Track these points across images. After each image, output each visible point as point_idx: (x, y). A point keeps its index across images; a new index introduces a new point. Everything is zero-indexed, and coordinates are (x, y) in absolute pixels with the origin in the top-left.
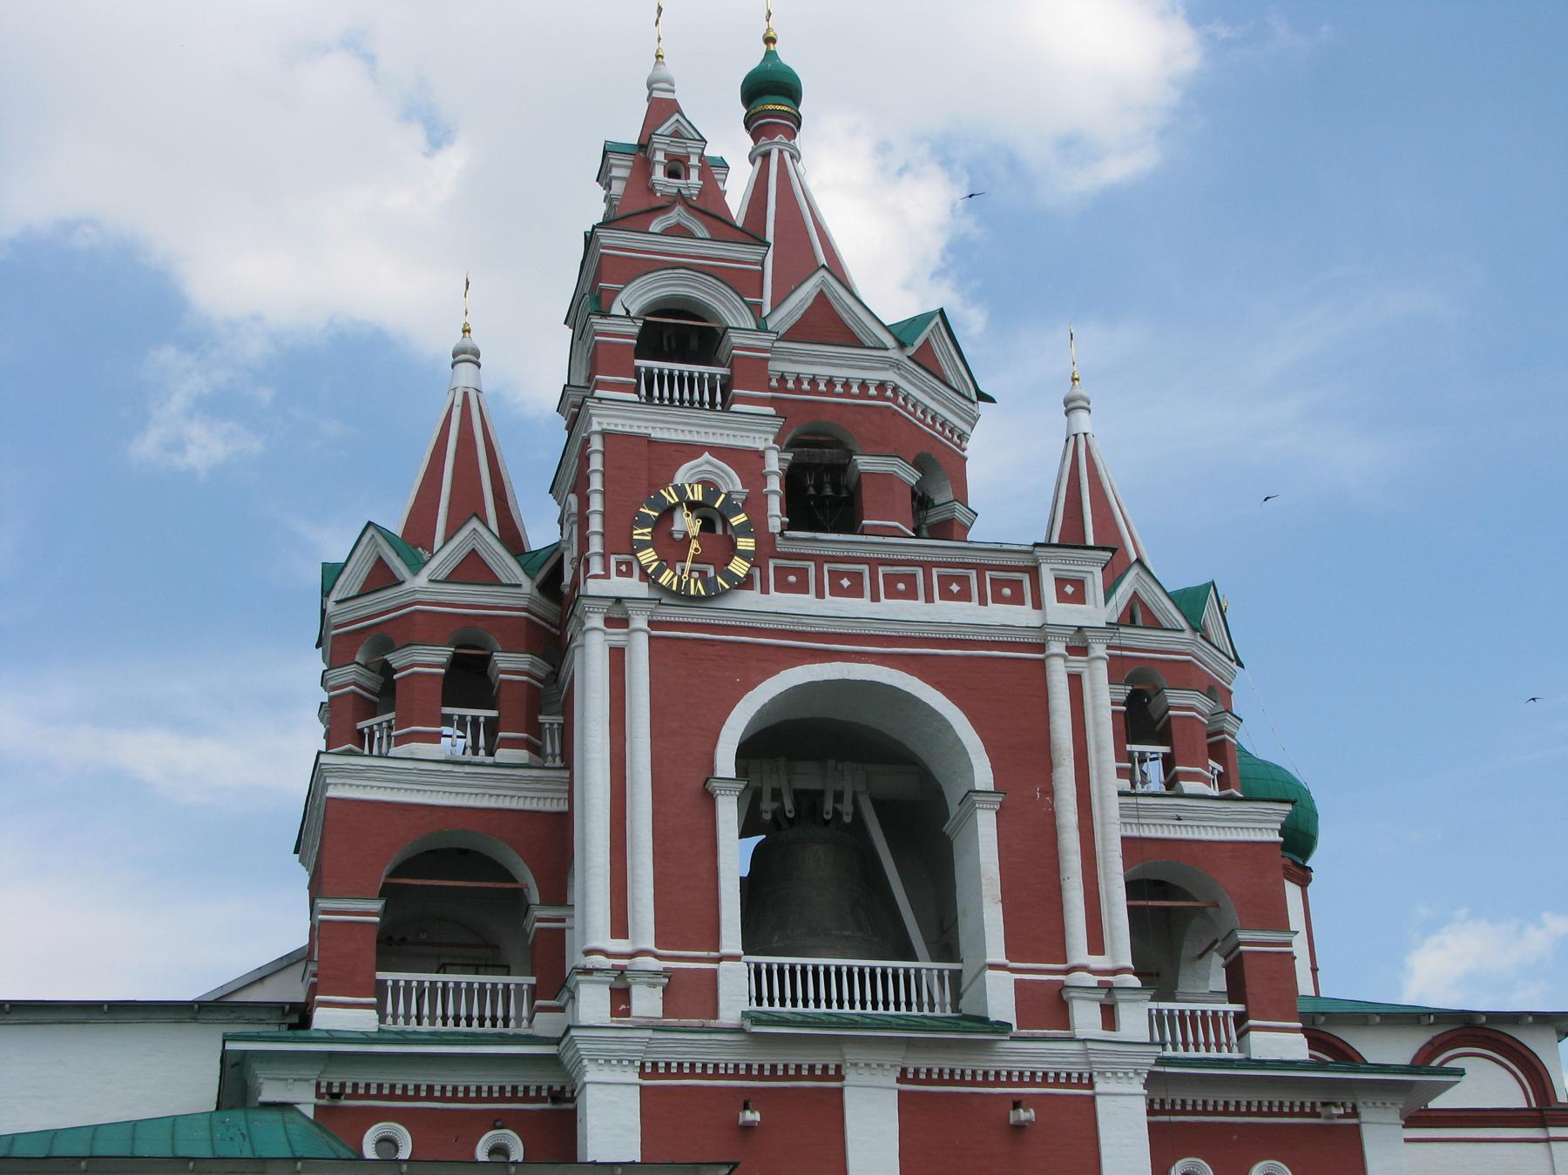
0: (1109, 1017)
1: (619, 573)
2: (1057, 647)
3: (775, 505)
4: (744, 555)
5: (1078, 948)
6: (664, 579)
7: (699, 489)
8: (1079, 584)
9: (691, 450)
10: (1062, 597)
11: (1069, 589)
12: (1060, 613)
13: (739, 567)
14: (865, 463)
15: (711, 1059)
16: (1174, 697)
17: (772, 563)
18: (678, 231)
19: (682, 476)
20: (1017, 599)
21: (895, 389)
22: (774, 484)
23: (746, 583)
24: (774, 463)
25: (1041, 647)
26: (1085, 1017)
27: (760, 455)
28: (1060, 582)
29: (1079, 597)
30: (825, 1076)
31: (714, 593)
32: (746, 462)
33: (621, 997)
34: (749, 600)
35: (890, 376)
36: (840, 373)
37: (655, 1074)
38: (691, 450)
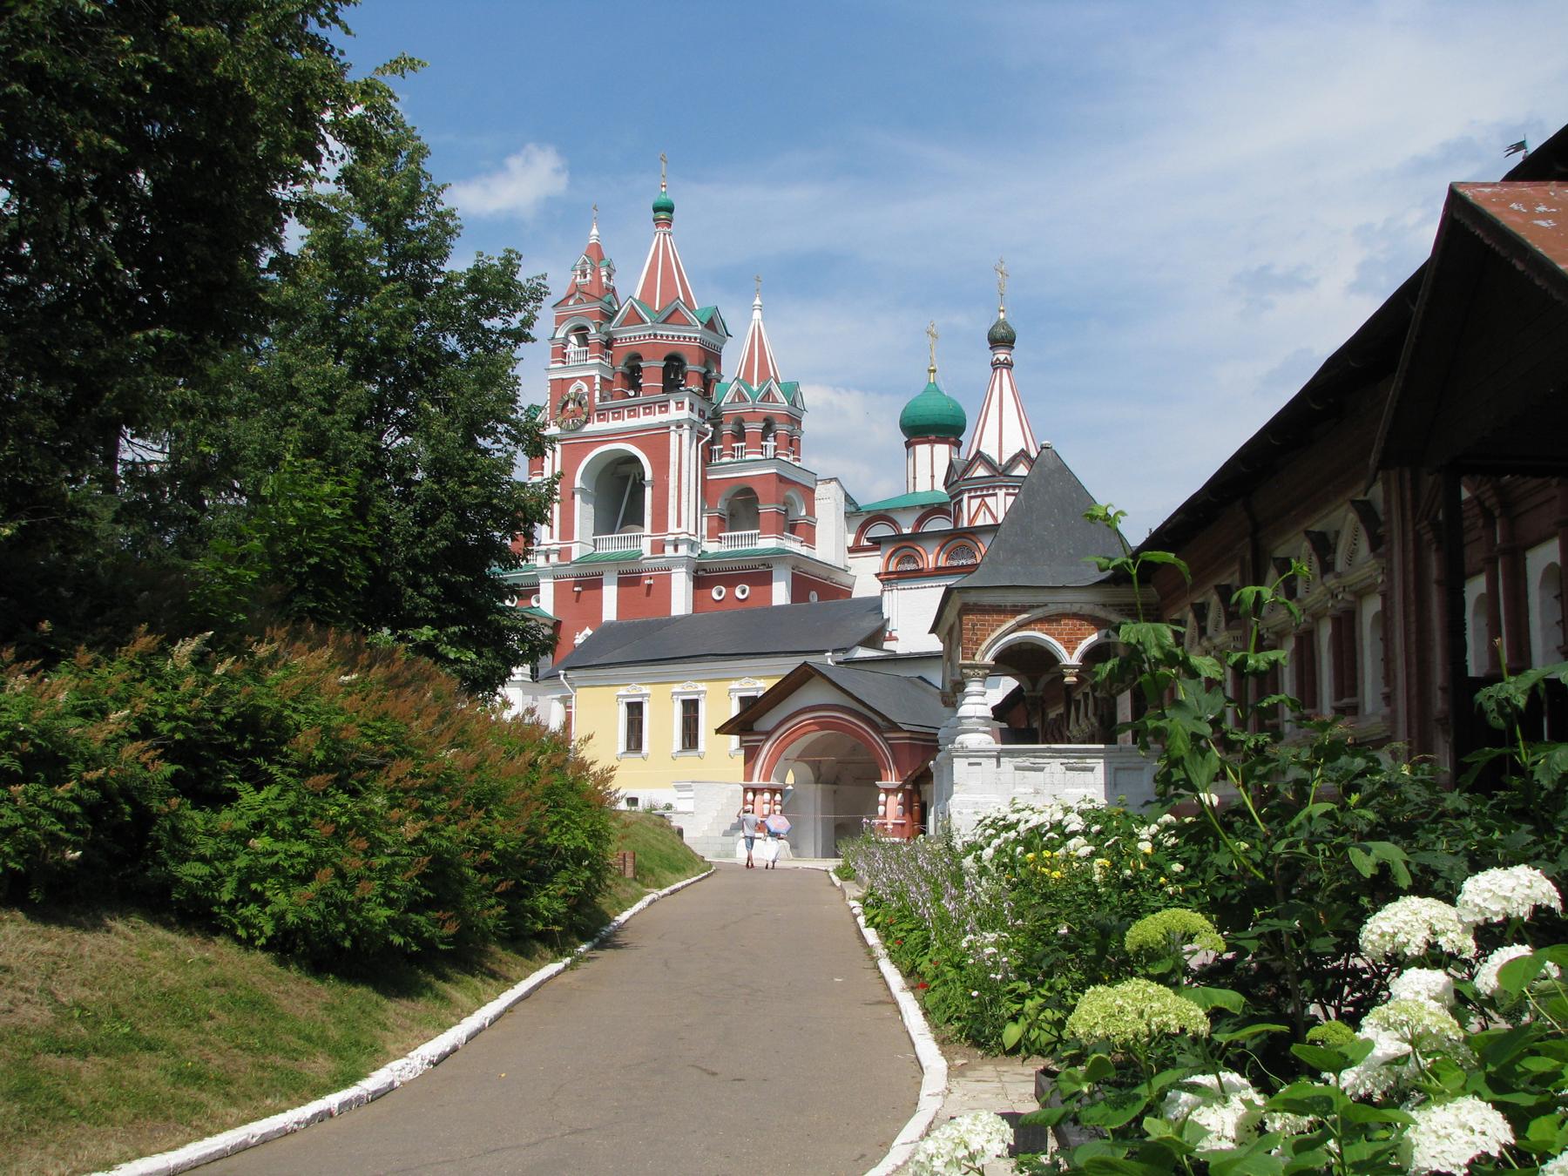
0: (676, 550)
3: (597, 394)
5: (672, 526)
13: (584, 418)
14: (642, 364)
16: (746, 425)
19: (572, 390)
23: (586, 422)
24: (598, 379)
26: (669, 550)
32: (589, 380)
33: (547, 558)
34: (589, 428)
38: (574, 379)
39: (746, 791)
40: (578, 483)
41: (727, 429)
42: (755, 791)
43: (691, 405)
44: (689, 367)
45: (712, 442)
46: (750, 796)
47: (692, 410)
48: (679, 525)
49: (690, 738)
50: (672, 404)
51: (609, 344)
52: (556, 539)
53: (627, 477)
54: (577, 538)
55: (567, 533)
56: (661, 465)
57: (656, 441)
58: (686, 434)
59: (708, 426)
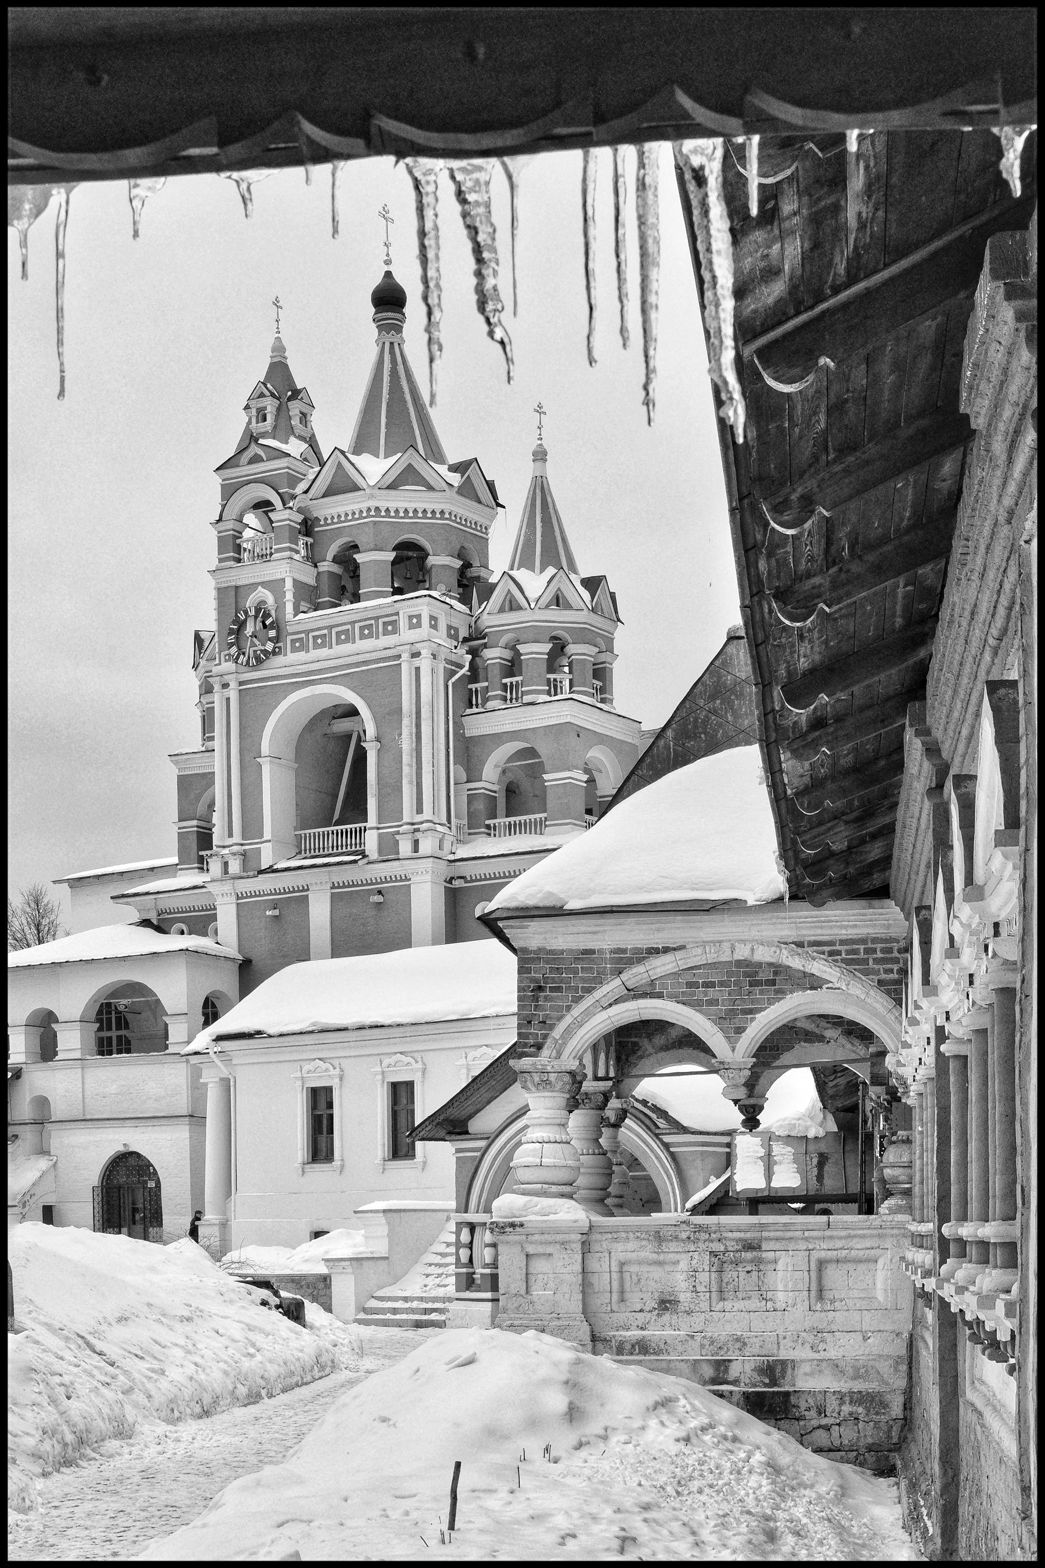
1: (226, 661)
2: (405, 656)
3: (289, 608)
4: (270, 639)
6: (240, 661)
7: (253, 609)
8: (419, 617)
9: (254, 586)
10: (412, 627)
11: (415, 621)
12: (407, 635)
13: (269, 646)
14: (359, 558)
15: (261, 888)
16: (522, 648)
17: (289, 638)
18: (256, 459)
19: (250, 602)
20: (395, 631)
21: (377, 509)
22: (289, 596)
24: (289, 584)
25: (399, 656)
26: (405, 847)
27: (283, 580)
28: (411, 617)
29: (419, 625)
30: (304, 890)
31: (259, 661)
32: (275, 586)
34: (279, 660)
35: (372, 504)
36: (349, 508)
37: (243, 898)
38: (254, 586)
39: (459, 1225)
40: (265, 748)
41: (494, 655)
42: (472, 1227)
43: (433, 618)
44: (432, 560)
45: (474, 675)
46: (465, 1236)
47: (434, 627)
48: (420, 810)
49: (400, 1147)
50: (403, 623)
51: (308, 527)
52: (237, 838)
53: (348, 736)
54: (267, 835)
55: (252, 827)
56: (390, 715)
57: (380, 679)
58: (425, 663)
59: (462, 650)
